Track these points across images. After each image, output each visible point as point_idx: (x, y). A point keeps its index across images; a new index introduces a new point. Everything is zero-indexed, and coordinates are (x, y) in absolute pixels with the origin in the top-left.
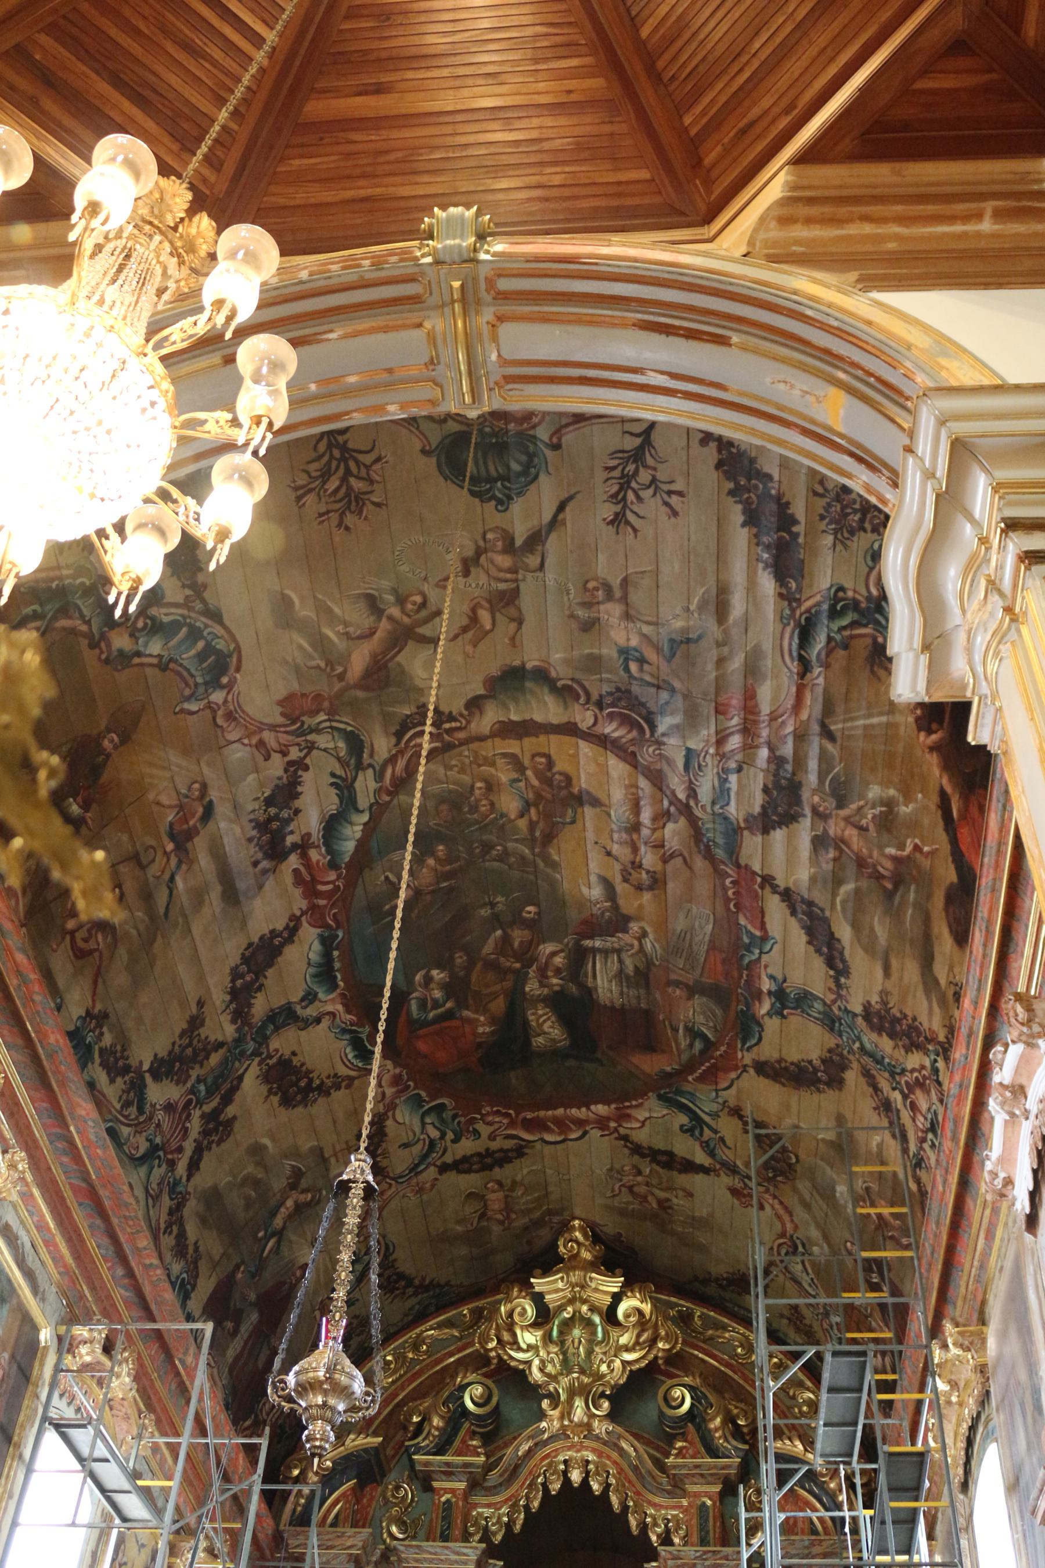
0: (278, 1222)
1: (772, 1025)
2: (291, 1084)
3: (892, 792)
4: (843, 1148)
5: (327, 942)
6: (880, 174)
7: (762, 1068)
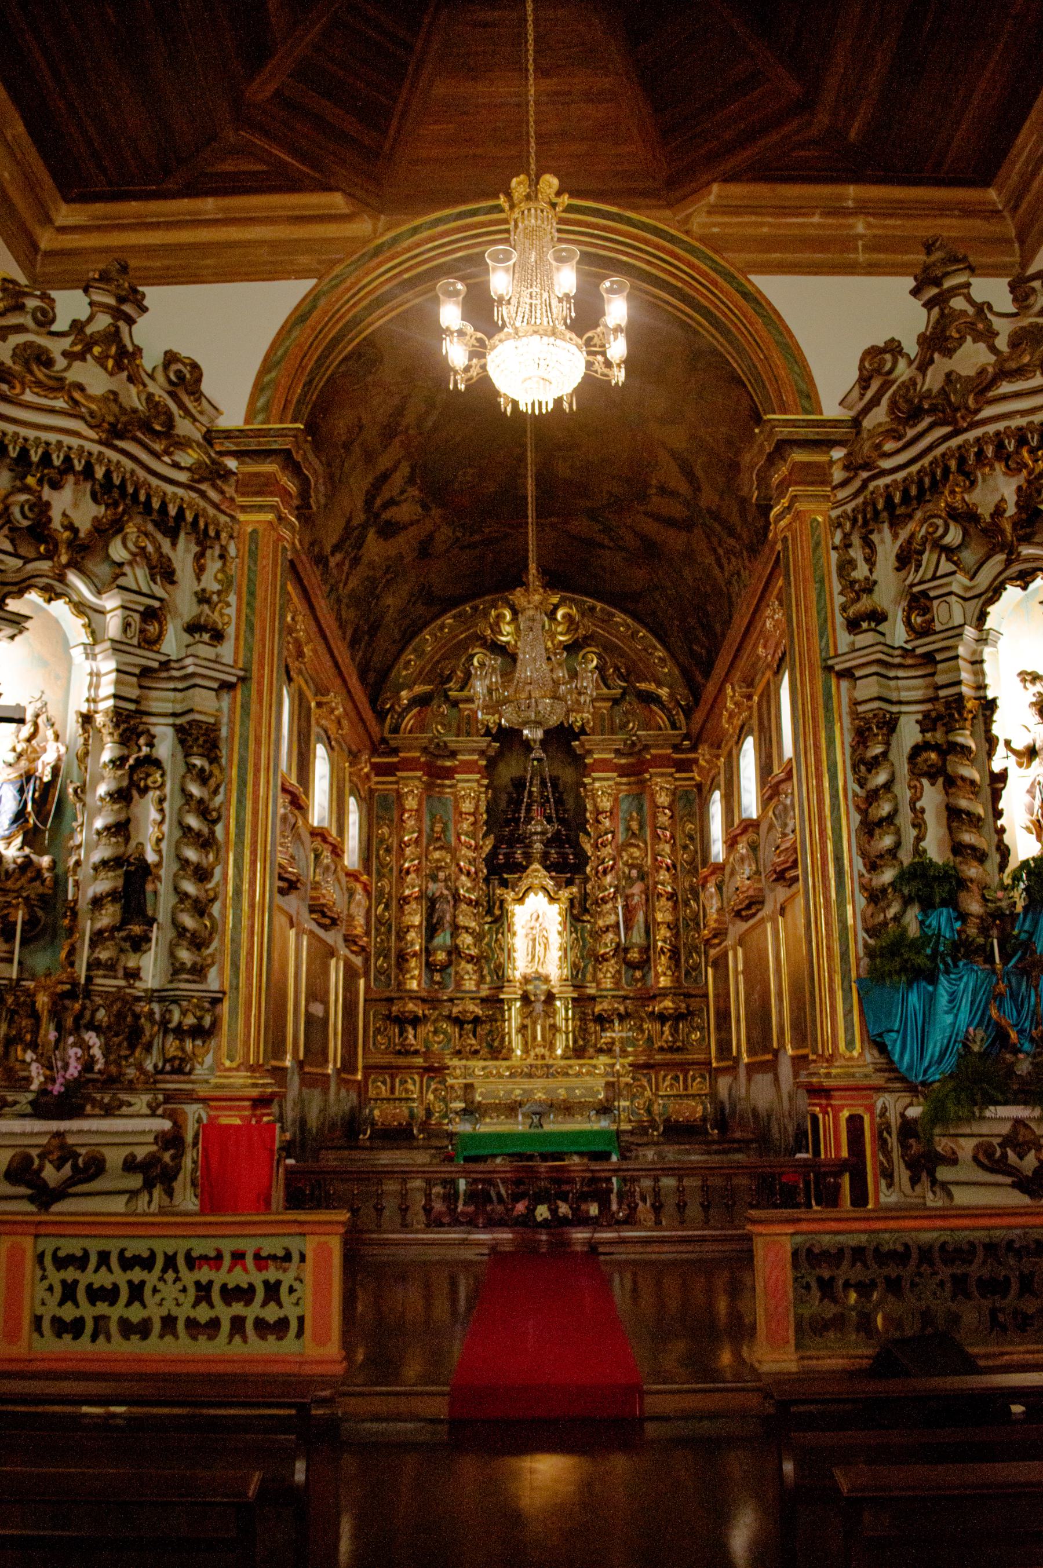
0: (377, 592)
1: (654, 498)
2: (389, 530)
3: (735, 434)
4: (689, 556)
5: (413, 468)
6: (763, 190)
7: (646, 513)
